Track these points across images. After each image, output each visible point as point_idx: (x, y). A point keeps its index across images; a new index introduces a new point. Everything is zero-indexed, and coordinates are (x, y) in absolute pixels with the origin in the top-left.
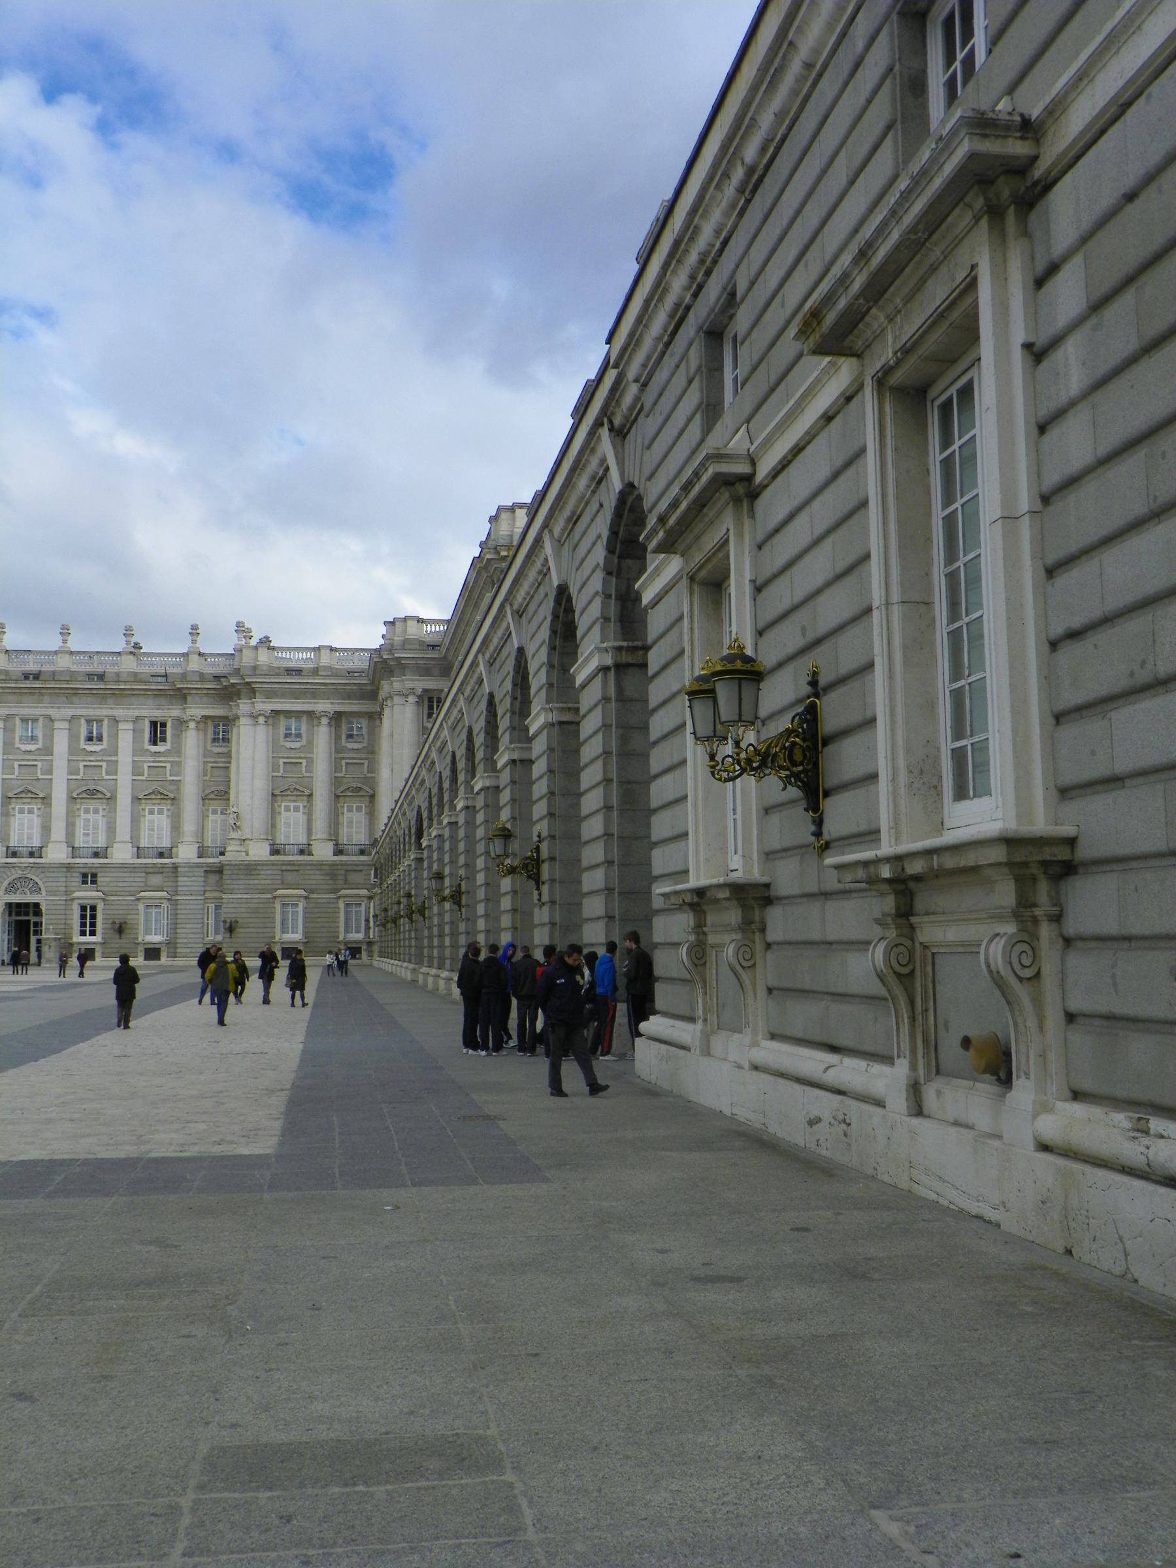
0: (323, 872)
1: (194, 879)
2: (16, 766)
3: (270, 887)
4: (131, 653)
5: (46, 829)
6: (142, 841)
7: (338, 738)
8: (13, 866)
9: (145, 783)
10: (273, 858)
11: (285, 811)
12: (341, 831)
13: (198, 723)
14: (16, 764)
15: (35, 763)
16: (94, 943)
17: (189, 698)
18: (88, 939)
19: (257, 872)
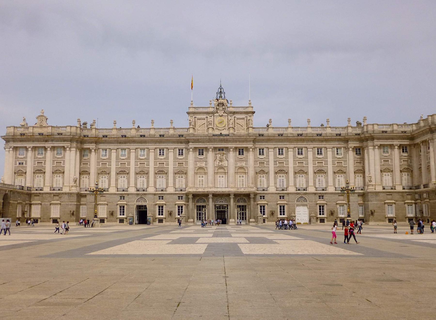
0: (399, 195)
1: (355, 197)
2: (297, 163)
3: (383, 200)
4: (330, 127)
5: (307, 182)
6: (336, 185)
7: (400, 153)
8: (299, 194)
9: (336, 167)
10: (384, 191)
11: (385, 176)
12: (403, 182)
13: (352, 148)
14: (297, 162)
15: (303, 162)
16: (325, 217)
17: (349, 141)
18: (322, 216)
19: (379, 195)
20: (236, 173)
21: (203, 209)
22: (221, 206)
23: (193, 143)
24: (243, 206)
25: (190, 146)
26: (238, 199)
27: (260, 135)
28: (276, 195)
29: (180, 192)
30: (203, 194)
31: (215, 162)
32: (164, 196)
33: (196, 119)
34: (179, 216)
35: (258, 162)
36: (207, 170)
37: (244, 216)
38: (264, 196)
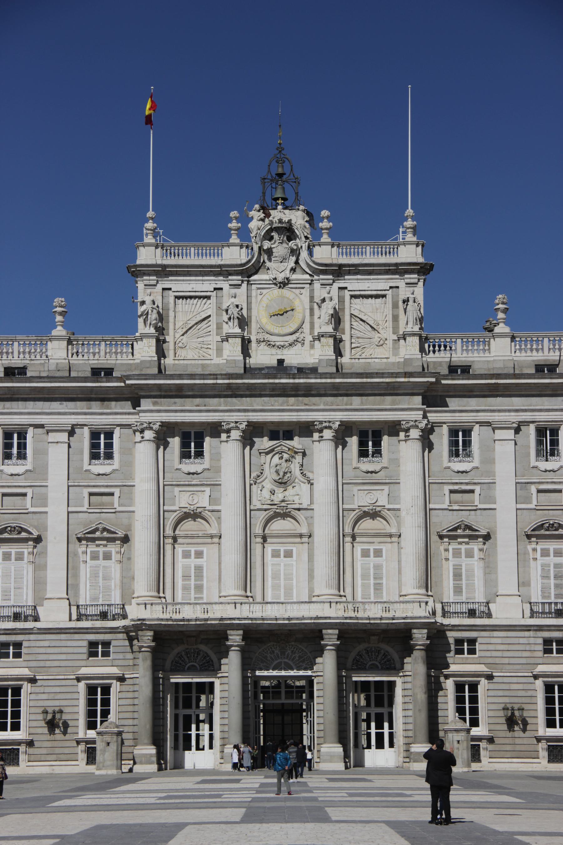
20: (348, 539)
21: (203, 697)
22: (283, 686)
23: (155, 404)
24: (379, 684)
25: (146, 418)
26: (359, 654)
27: (453, 370)
28: (527, 634)
29: (99, 624)
30: (201, 632)
31: (254, 487)
32: (25, 644)
33: (172, 300)
34: (92, 734)
35: (447, 488)
36: (219, 524)
37: (386, 731)
38: (472, 642)
